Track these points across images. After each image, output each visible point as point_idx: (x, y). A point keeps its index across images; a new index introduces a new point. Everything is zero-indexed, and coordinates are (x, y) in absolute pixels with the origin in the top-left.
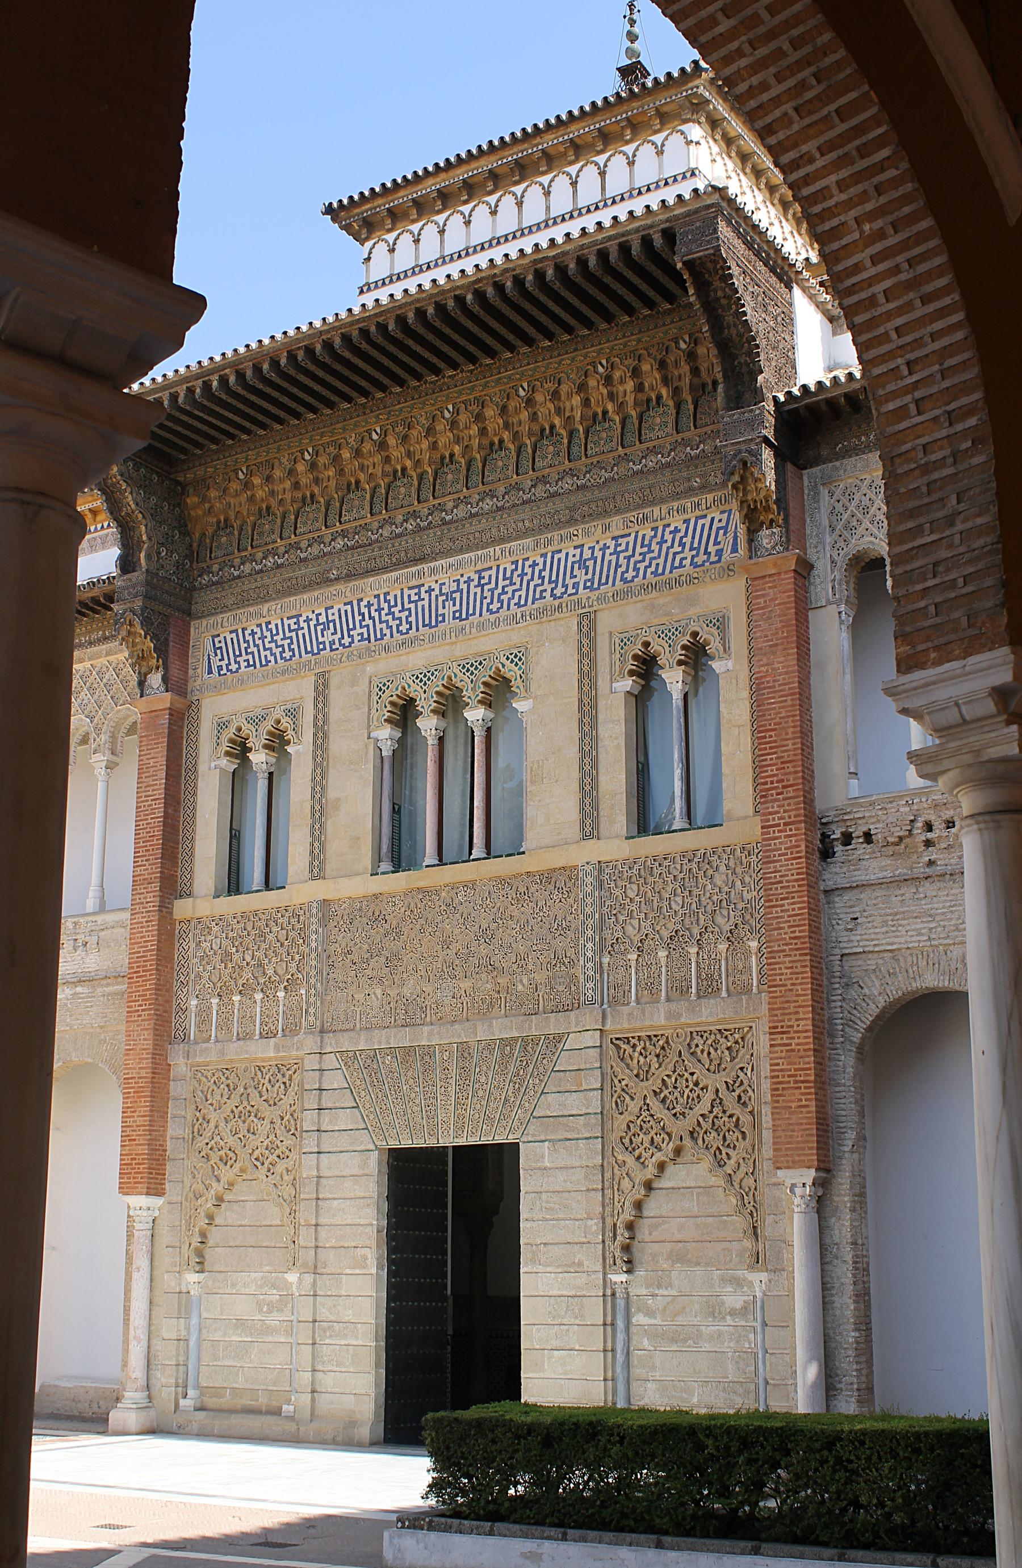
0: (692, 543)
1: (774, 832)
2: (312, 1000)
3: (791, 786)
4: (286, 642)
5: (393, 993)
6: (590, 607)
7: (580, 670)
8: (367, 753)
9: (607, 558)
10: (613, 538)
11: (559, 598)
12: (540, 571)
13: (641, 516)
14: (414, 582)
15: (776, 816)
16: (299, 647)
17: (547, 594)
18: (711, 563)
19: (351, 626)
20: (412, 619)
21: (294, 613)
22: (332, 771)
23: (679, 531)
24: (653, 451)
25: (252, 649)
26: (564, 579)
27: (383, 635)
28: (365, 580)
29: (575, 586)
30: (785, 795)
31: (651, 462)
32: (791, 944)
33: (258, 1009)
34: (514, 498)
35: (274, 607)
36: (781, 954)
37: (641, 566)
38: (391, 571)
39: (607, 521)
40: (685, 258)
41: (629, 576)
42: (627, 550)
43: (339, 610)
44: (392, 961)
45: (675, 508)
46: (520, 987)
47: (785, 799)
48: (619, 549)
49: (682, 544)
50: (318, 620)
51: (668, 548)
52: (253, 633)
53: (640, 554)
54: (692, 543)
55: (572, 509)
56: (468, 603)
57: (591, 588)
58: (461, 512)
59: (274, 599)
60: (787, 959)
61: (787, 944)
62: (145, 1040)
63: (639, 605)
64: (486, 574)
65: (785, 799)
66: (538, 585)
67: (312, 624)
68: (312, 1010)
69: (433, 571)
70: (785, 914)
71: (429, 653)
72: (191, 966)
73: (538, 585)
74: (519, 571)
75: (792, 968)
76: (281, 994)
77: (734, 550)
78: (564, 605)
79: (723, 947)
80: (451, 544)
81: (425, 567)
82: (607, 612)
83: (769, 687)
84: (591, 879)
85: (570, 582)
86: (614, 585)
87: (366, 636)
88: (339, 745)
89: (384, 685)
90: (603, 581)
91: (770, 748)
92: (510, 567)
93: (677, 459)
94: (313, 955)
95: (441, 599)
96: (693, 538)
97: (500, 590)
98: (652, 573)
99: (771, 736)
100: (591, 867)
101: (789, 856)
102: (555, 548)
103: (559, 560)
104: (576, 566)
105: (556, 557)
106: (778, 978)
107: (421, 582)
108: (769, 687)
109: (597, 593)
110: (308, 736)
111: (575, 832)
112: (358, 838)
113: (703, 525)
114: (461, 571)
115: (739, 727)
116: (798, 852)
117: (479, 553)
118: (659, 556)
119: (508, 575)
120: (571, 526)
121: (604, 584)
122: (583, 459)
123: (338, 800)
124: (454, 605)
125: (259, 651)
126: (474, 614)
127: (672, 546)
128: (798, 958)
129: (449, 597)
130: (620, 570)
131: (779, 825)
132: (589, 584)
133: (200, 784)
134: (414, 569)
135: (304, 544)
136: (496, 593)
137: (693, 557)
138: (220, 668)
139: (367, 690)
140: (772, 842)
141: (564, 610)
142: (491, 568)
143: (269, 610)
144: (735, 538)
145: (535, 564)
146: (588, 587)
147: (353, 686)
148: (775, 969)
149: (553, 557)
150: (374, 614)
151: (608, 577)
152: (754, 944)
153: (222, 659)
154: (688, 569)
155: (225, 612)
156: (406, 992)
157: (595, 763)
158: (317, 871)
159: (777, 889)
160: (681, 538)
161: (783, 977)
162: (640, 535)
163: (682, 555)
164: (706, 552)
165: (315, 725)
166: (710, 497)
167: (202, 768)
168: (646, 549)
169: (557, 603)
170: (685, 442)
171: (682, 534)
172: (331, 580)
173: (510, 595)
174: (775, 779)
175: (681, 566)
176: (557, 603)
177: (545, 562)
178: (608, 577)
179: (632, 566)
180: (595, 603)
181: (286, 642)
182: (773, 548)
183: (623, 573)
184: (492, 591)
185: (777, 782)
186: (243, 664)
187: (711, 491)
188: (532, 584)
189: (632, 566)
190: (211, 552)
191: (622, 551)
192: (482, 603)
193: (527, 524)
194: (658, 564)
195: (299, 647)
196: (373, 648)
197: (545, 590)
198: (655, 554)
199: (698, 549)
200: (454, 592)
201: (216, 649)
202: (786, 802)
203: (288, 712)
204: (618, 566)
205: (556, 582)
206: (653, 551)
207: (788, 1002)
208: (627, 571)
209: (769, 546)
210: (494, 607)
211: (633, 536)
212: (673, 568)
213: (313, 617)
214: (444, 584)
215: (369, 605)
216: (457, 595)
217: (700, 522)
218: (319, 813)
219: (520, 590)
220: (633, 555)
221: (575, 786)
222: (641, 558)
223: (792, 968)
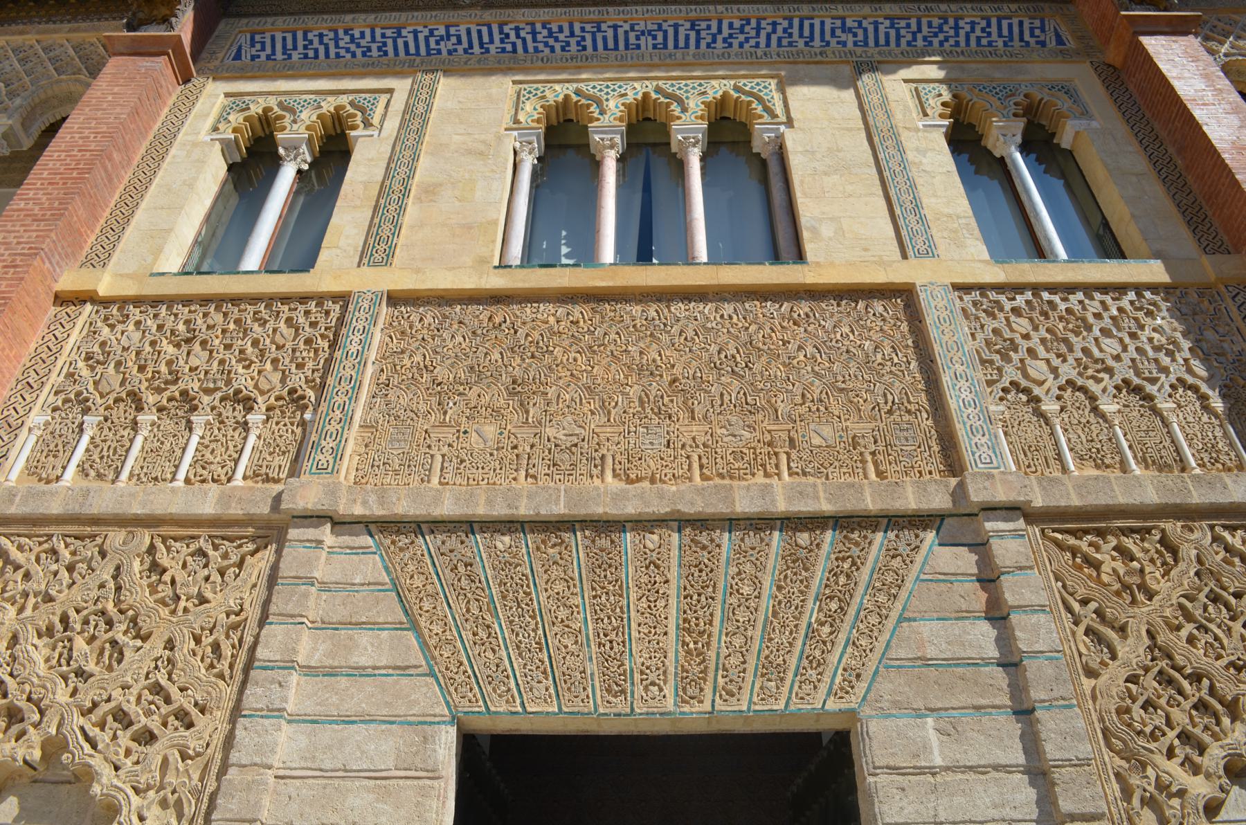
37: (936, 41)
67: (421, 37)
77: (1060, 41)
85: (833, 42)
86: (898, 45)
92: (737, 24)
105: (807, 23)
109: (877, 49)
118: (957, 35)
126: (687, 46)
144: (1058, 36)
155: (282, 14)
162: (924, 21)
169: (818, 51)
188: (774, 38)
204: (898, 37)
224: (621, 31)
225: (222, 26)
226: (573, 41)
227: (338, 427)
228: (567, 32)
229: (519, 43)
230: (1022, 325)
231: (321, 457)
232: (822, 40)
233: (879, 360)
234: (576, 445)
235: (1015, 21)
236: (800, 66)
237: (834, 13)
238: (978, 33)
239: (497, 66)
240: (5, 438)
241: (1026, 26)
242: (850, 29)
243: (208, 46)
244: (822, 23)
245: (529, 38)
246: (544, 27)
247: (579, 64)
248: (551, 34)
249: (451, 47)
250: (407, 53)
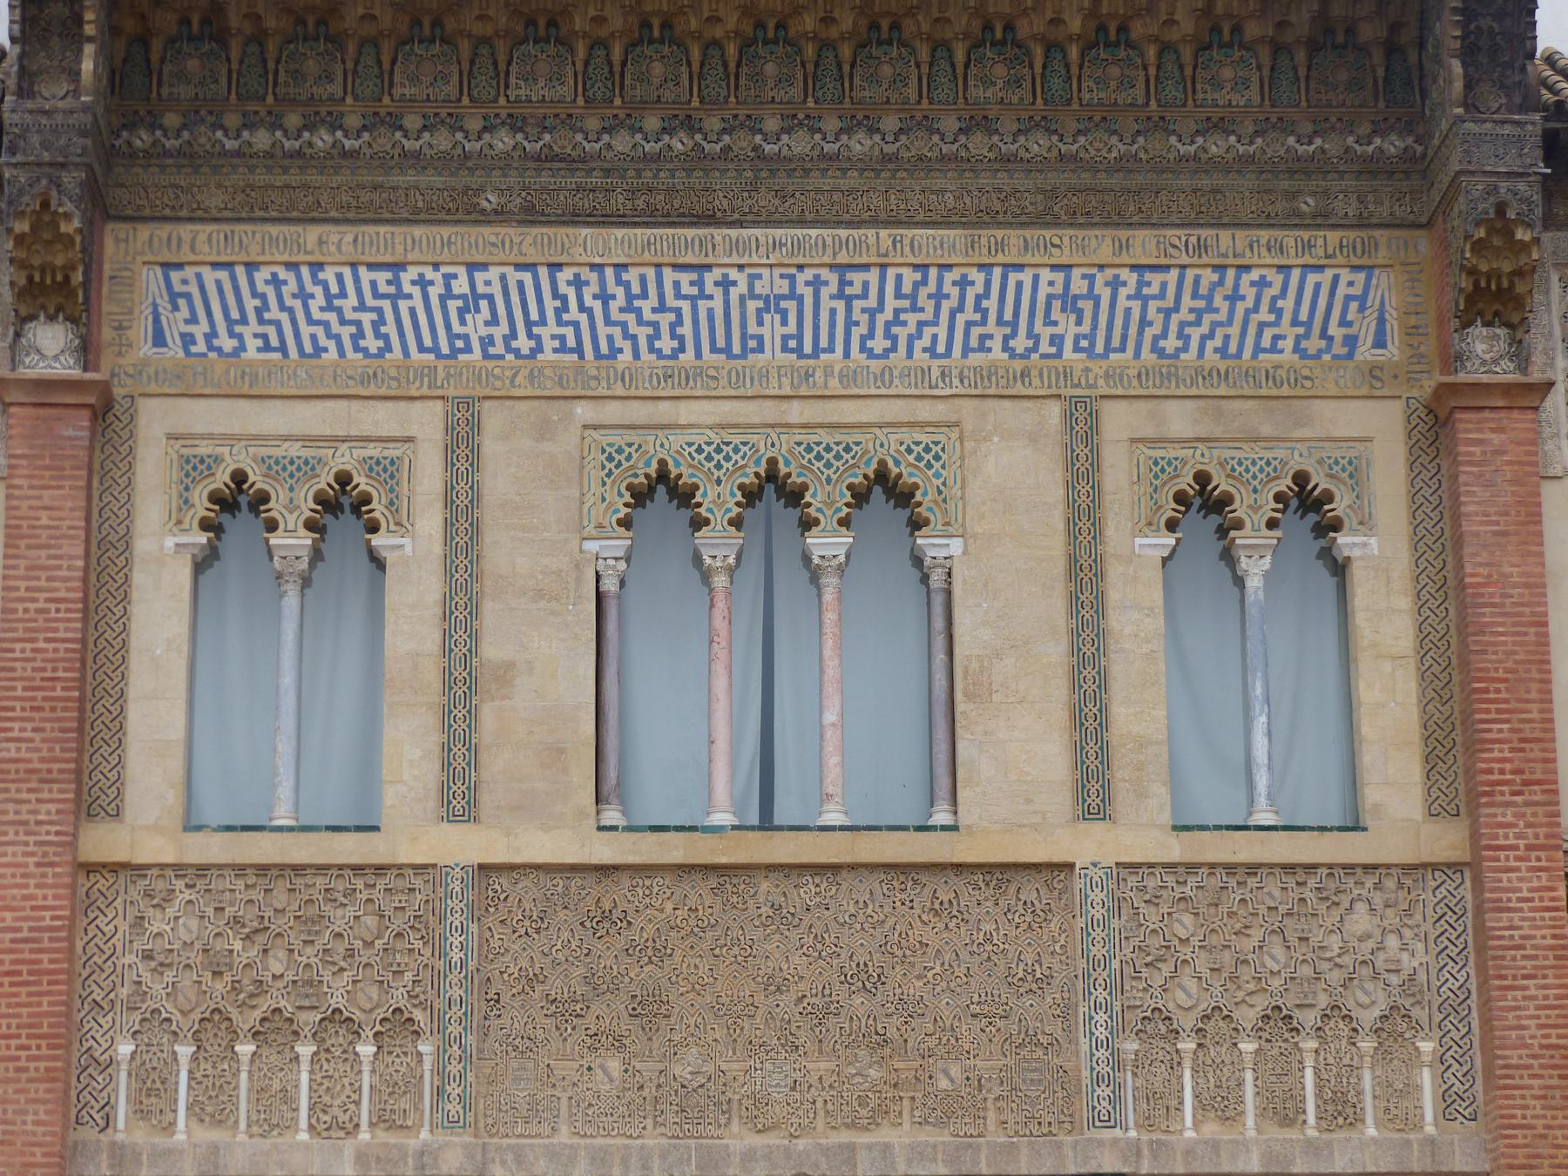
0: (1296, 312)
1: (1507, 859)
2: (454, 1068)
3: (1538, 782)
4: (367, 318)
5: (648, 1068)
6: (1090, 386)
7: (1071, 503)
8: (579, 580)
9: (1122, 302)
10: (1134, 267)
11: (1022, 356)
12: (979, 298)
13: (1193, 240)
14: (690, 259)
15: (1511, 832)
16: (401, 334)
17: (996, 345)
18: (1335, 357)
19: (534, 316)
20: (686, 330)
21: (388, 259)
22: (489, 608)
23: (1270, 284)
24: (1219, 125)
25: (274, 313)
26: (1031, 324)
27: (615, 352)
28: (571, 231)
29: (1057, 340)
30: (1526, 797)
31: (1216, 146)
32: (1543, 1057)
33: (304, 1077)
34: (920, 144)
35: (335, 238)
36: (1525, 1073)
37: (1195, 334)
38: (635, 225)
39: (1123, 234)
41: (1171, 344)
42: (1162, 295)
43: (503, 278)
44: (648, 1009)
45: (1263, 241)
46: (944, 1083)
47: (1527, 804)
48: (1146, 291)
49: (1273, 309)
50: (448, 286)
51: (1248, 312)
52: (275, 281)
53: (1191, 310)
54: (1296, 312)
55: (1052, 194)
56: (816, 328)
57: (1090, 351)
58: (799, 144)
59: (335, 221)
60: (1535, 1082)
61: (1534, 1057)
62: (37, 1123)
63: (1189, 404)
64: (857, 278)
65: (1527, 804)
66: (975, 323)
67: (435, 292)
68: (453, 1089)
69: (735, 246)
70: (1531, 1004)
71: (727, 406)
72: (119, 969)
73: (975, 323)
74: (932, 287)
75: (1545, 1097)
76: (366, 1050)
77: (1380, 343)
78: (1034, 373)
79: (1367, 1044)
80: (777, 202)
81: (718, 234)
82: (1123, 405)
83: (1493, 605)
84: (1102, 896)
86: (1137, 355)
87: (571, 342)
88: (505, 552)
89: (620, 451)
90: (1116, 343)
91: (1498, 711)
93: (1270, 152)
94: (454, 977)
95: (752, 306)
96: (1298, 302)
97: (888, 314)
98: (1216, 350)
99: (1498, 691)
100: (1101, 873)
101: (1537, 904)
102: (1008, 260)
103: (1019, 285)
104: (1057, 304)
106: (1519, 1112)
107: (703, 260)
108: (1493, 605)
109: (1105, 364)
110: (429, 523)
111: (1060, 801)
112: (561, 751)
113: (1318, 286)
114: (800, 260)
115: (1394, 658)
116: (1552, 899)
117: (843, 233)
118: (1230, 322)
119: (907, 288)
120: (1046, 225)
121: (1115, 350)
122: (1075, 106)
123: (510, 665)
124: (784, 322)
125: (294, 322)
126: (831, 349)
127: (1256, 309)
128: (1555, 1082)
129: (771, 304)
130: (1149, 332)
131: (1516, 848)
132: (1084, 343)
133: (139, 577)
134: (690, 233)
135: (412, 122)
136: (881, 319)
137: (1298, 339)
138: (188, 340)
139: (577, 455)
140: (1504, 876)
141: (1036, 382)
142: (866, 267)
143: (321, 242)
144: (1381, 321)
145: (963, 283)
146: (1082, 350)
147: (541, 437)
148: (1512, 1097)
149: (1004, 278)
150: (588, 301)
151: (1124, 338)
152: (1427, 1046)
153: (193, 320)
154: (1287, 356)
155: (202, 220)
156: (681, 1071)
157: (1103, 683)
158: (459, 799)
159: (1514, 959)
160: (1274, 299)
161: (1529, 1113)
163: (1276, 331)
164: (1323, 334)
165: (448, 502)
166: (1334, 236)
167: (143, 545)
168: (1201, 304)
169: (1018, 365)
170: (1284, 126)
171: (1275, 290)
172: (483, 212)
173: (912, 328)
174: (1508, 766)
175: (1274, 349)
176: (1018, 365)
177: (988, 283)
178: (1124, 338)
179: (1173, 327)
180: (1101, 382)
181: (367, 318)
182: (1495, 362)
183: (1156, 339)
184: (872, 313)
185: (1513, 772)
186: (252, 344)
188: (961, 319)
189: (1173, 327)
190: (159, 84)
191: (1154, 297)
192: (848, 334)
193: (951, 203)
194: (1227, 337)
195: (401, 334)
196: (594, 372)
197: (991, 337)
198: (1222, 316)
199: (1308, 325)
200: (784, 297)
201: (173, 297)
202: (1529, 811)
203: (374, 467)
204: (1144, 322)
205: (1014, 324)
206: (1217, 311)
207: (1538, 1156)
208: (1164, 335)
209: (1487, 357)
210: (879, 344)
211: (1174, 273)
212: (1258, 349)
213: (437, 277)
214: (759, 277)
215: (578, 283)
216: (791, 306)
217: (1312, 278)
218: (463, 685)
219: (936, 324)
220: (1177, 309)
221: (1059, 715)
222: (1192, 317)
223: (1545, 1097)
224: (734, 293)
225: (109, 242)
226: (666, 319)
227: (460, 1067)
228: (653, 301)
229: (583, 318)
230: (1185, 924)
231: (448, 1107)
232: (1030, 334)
233: (1021, 975)
234: (702, 1086)
236: (990, 403)
237: (1059, 257)
238: (1264, 315)
239: (557, 392)
240: (100, 1079)
241: (1342, 290)
242: (1076, 298)
243: (105, 308)
244: (1036, 278)
245: (597, 306)
246: (619, 282)
247: (676, 393)
248: (630, 297)
249: (484, 331)
250: (422, 349)
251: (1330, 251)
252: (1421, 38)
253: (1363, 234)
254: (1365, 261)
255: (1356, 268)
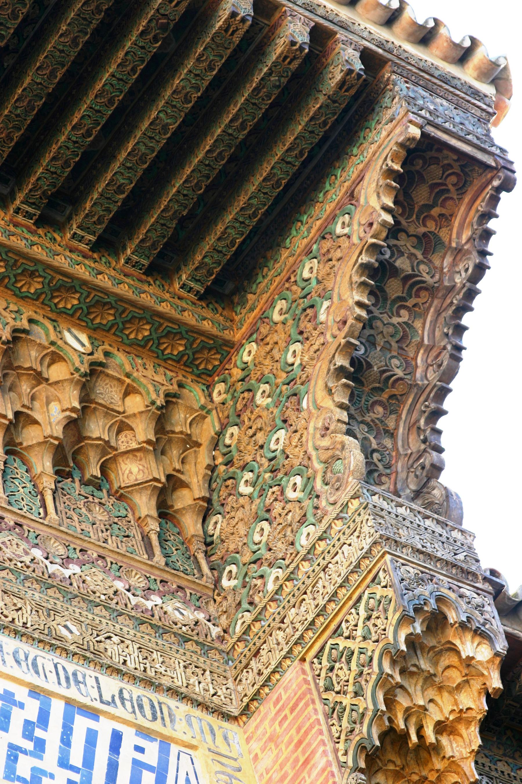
40: (429, 129)
166: (111, 685)
187: (113, 670)
235: (104, 728)
251: (107, 697)
252: (209, 501)
253: (156, 697)
254: (157, 726)
255: (143, 732)
